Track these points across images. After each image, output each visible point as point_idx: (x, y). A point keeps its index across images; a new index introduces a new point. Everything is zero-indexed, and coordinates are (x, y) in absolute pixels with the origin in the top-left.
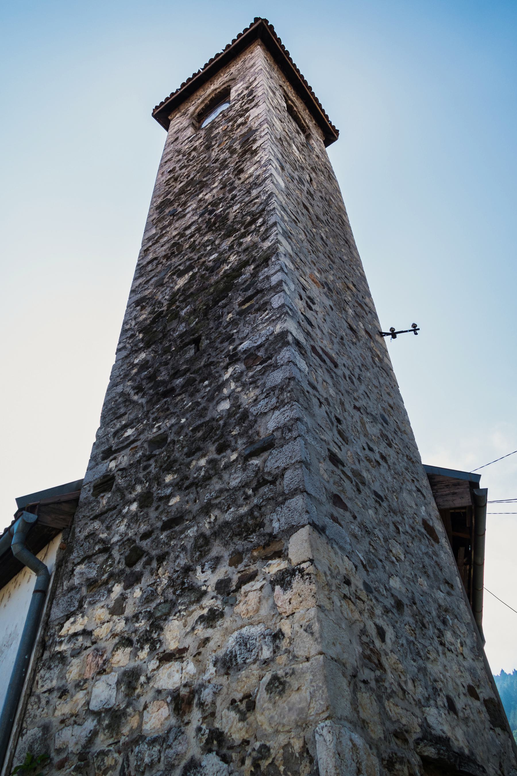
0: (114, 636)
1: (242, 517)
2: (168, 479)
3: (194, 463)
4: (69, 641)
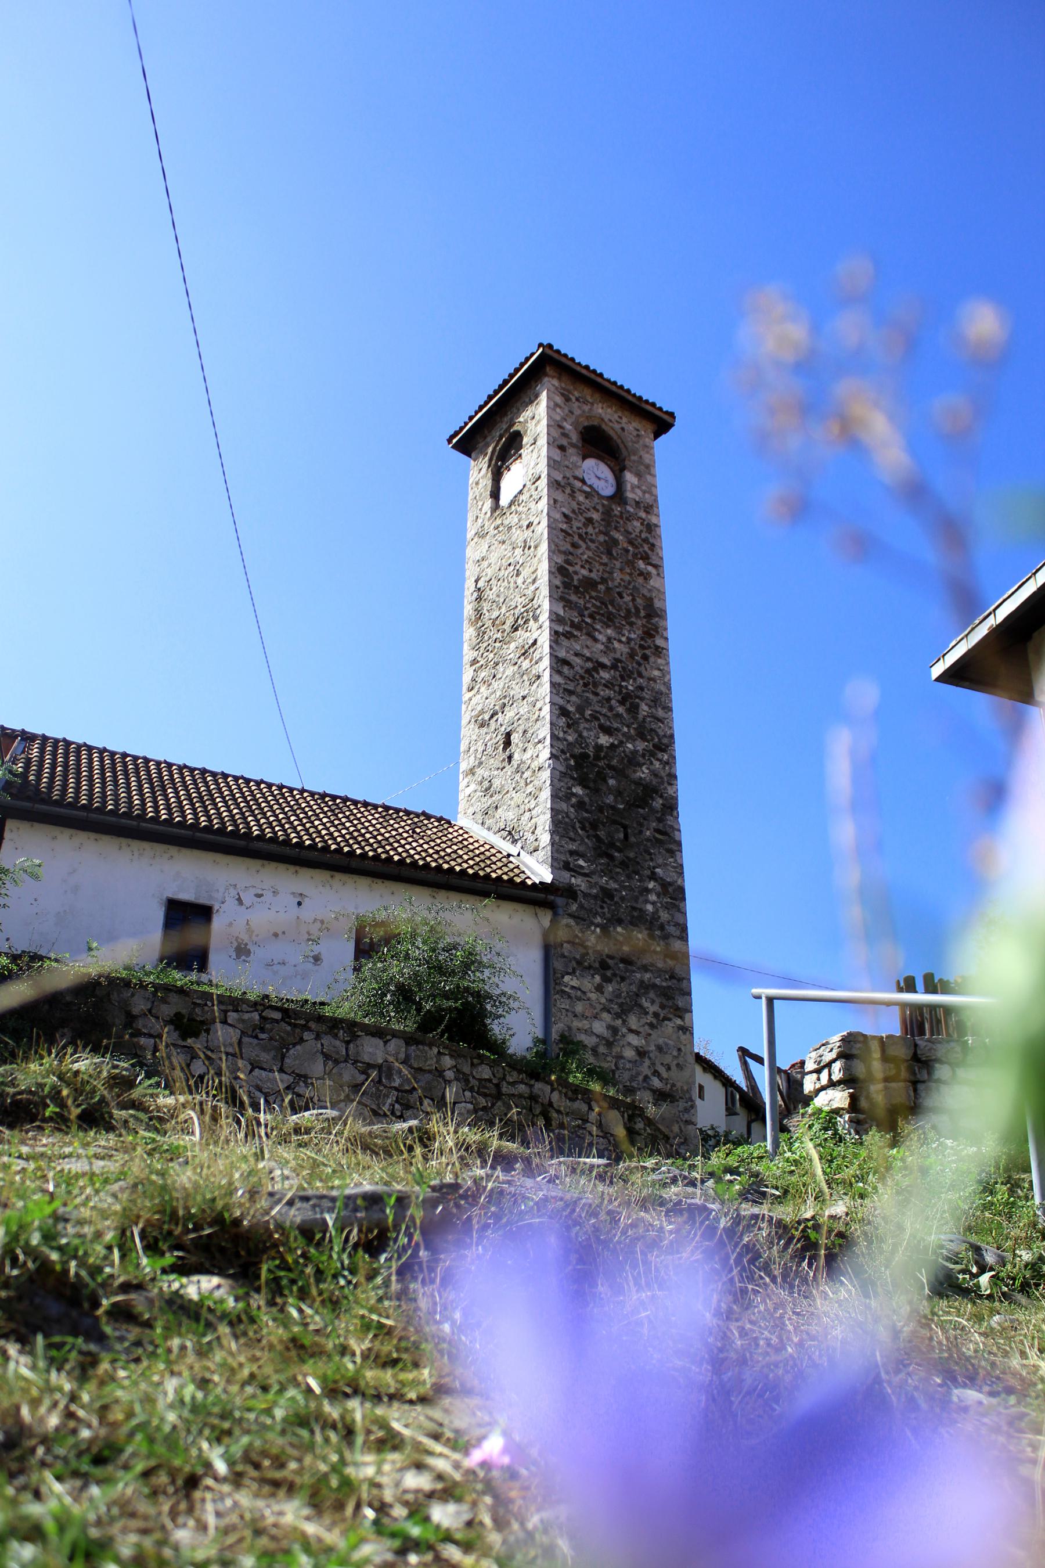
1: (664, 987)
2: (619, 929)
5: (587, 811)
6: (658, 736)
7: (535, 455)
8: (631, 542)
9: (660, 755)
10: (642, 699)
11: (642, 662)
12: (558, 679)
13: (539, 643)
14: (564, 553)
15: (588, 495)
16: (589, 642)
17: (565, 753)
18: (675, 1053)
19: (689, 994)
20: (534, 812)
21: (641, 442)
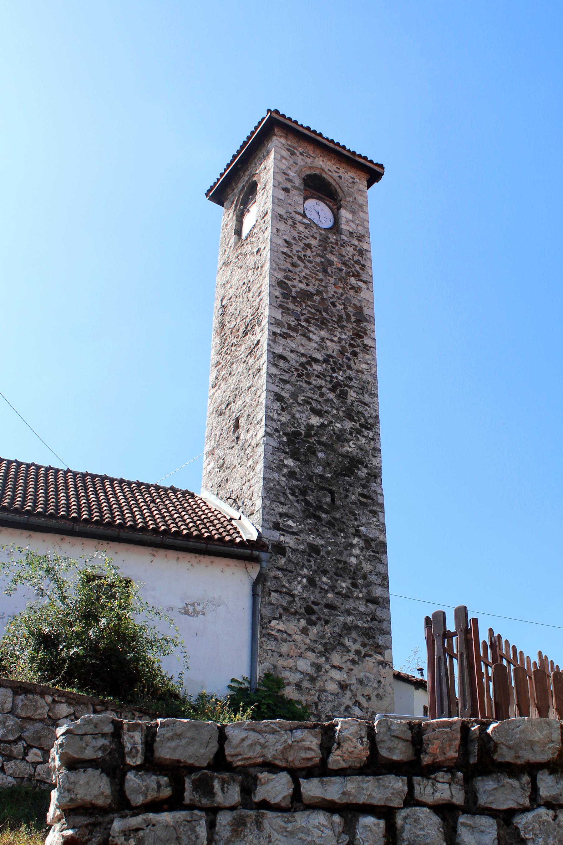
2: (324, 579)
3: (339, 582)
5: (297, 480)
6: (364, 417)
7: (265, 196)
8: (344, 264)
9: (366, 433)
10: (350, 387)
11: (351, 357)
12: (274, 371)
13: (260, 343)
14: (284, 270)
15: (307, 226)
16: (305, 341)
17: (279, 432)
18: (375, 685)
19: (389, 633)
20: (252, 482)
21: (356, 187)
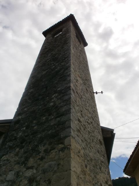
0: (15, 161)
2: (35, 122)
3: (42, 118)
4: (3, 162)
